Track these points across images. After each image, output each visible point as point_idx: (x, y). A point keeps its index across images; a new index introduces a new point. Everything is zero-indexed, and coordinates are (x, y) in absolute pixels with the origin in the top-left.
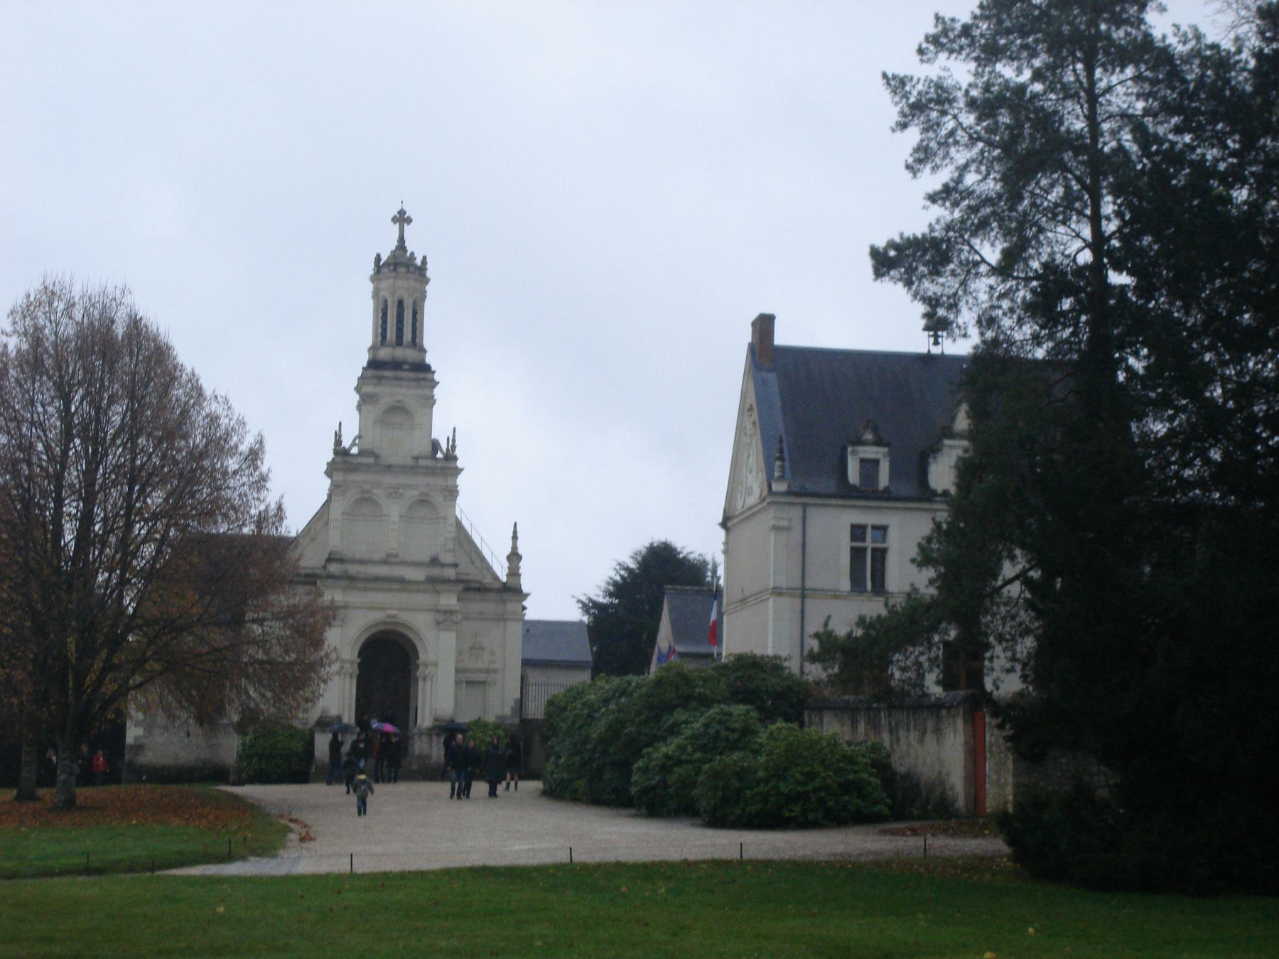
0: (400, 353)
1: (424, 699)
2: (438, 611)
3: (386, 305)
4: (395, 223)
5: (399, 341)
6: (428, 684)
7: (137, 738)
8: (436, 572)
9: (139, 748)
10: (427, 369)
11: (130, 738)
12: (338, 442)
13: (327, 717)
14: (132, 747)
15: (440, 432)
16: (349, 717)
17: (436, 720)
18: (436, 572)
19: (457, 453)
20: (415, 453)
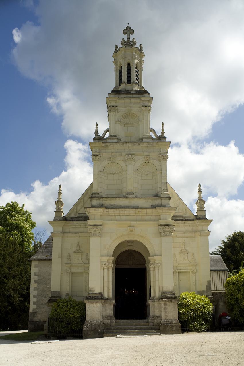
0: (129, 87)
1: (154, 281)
2: (161, 225)
3: (121, 68)
4: (125, 34)
5: (129, 81)
6: (157, 270)
7: (34, 309)
8: (157, 201)
9: (35, 313)
10: (146, 92)
11: (31, 310)
12: (97, 133)
13: (93, 294)
14: (32, 313)
15: (155, 124)
16: (108, 293)
17: (163, 293)
18: (157, 201)
19: (165, 135)
20: (141, 137)
